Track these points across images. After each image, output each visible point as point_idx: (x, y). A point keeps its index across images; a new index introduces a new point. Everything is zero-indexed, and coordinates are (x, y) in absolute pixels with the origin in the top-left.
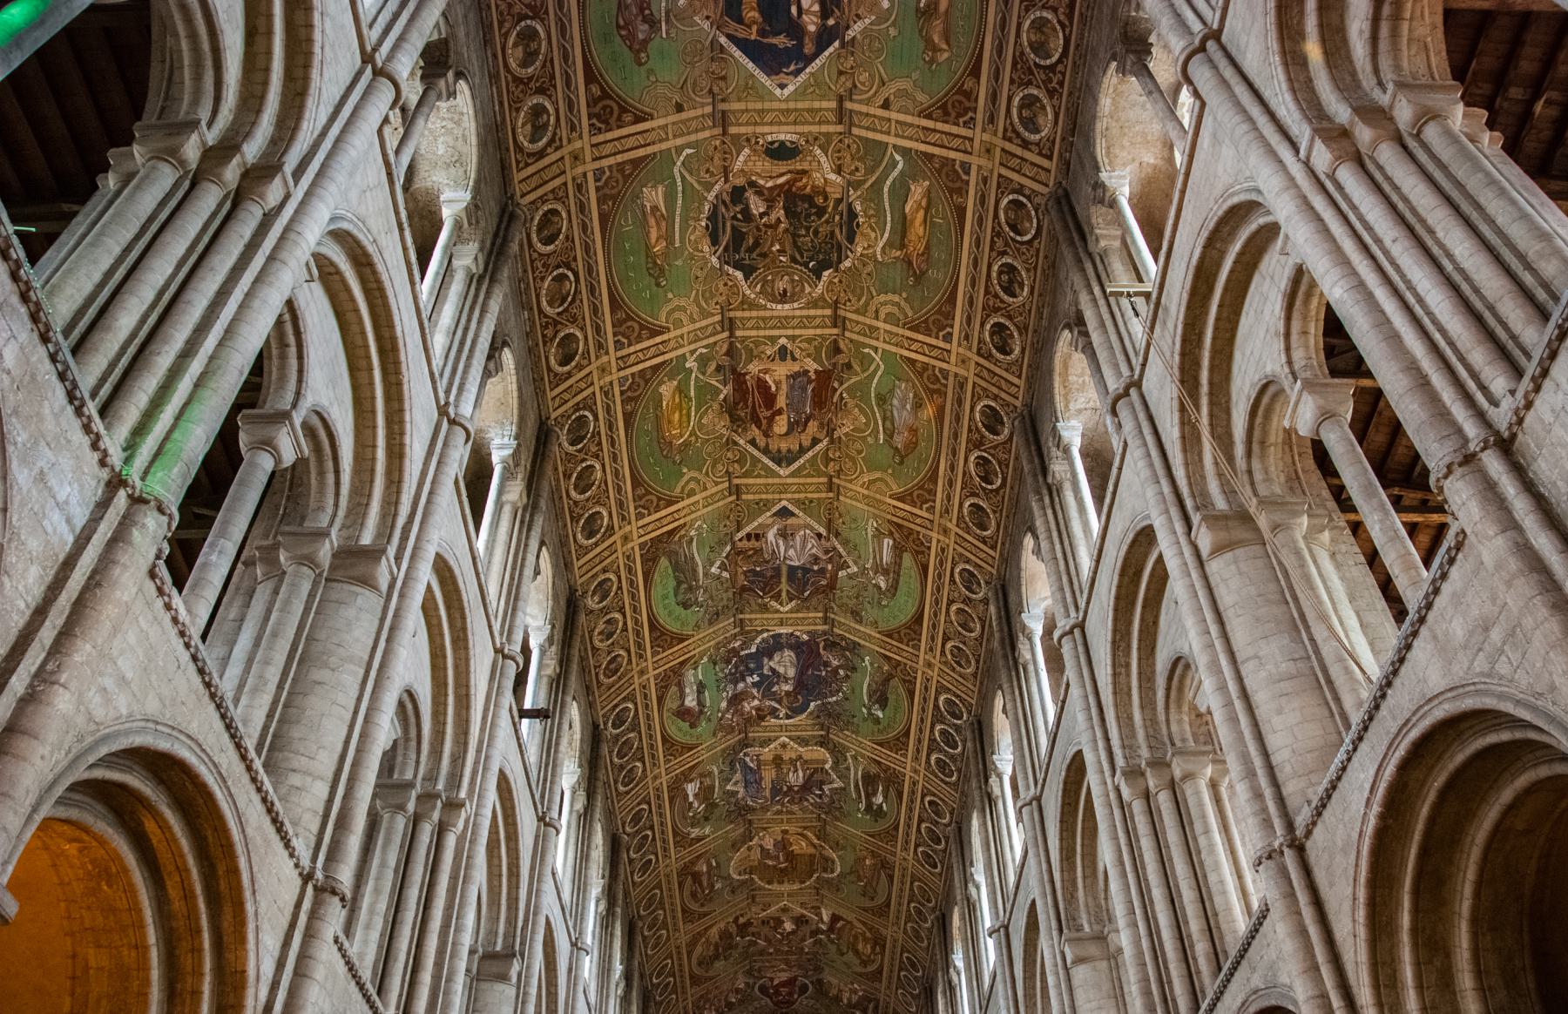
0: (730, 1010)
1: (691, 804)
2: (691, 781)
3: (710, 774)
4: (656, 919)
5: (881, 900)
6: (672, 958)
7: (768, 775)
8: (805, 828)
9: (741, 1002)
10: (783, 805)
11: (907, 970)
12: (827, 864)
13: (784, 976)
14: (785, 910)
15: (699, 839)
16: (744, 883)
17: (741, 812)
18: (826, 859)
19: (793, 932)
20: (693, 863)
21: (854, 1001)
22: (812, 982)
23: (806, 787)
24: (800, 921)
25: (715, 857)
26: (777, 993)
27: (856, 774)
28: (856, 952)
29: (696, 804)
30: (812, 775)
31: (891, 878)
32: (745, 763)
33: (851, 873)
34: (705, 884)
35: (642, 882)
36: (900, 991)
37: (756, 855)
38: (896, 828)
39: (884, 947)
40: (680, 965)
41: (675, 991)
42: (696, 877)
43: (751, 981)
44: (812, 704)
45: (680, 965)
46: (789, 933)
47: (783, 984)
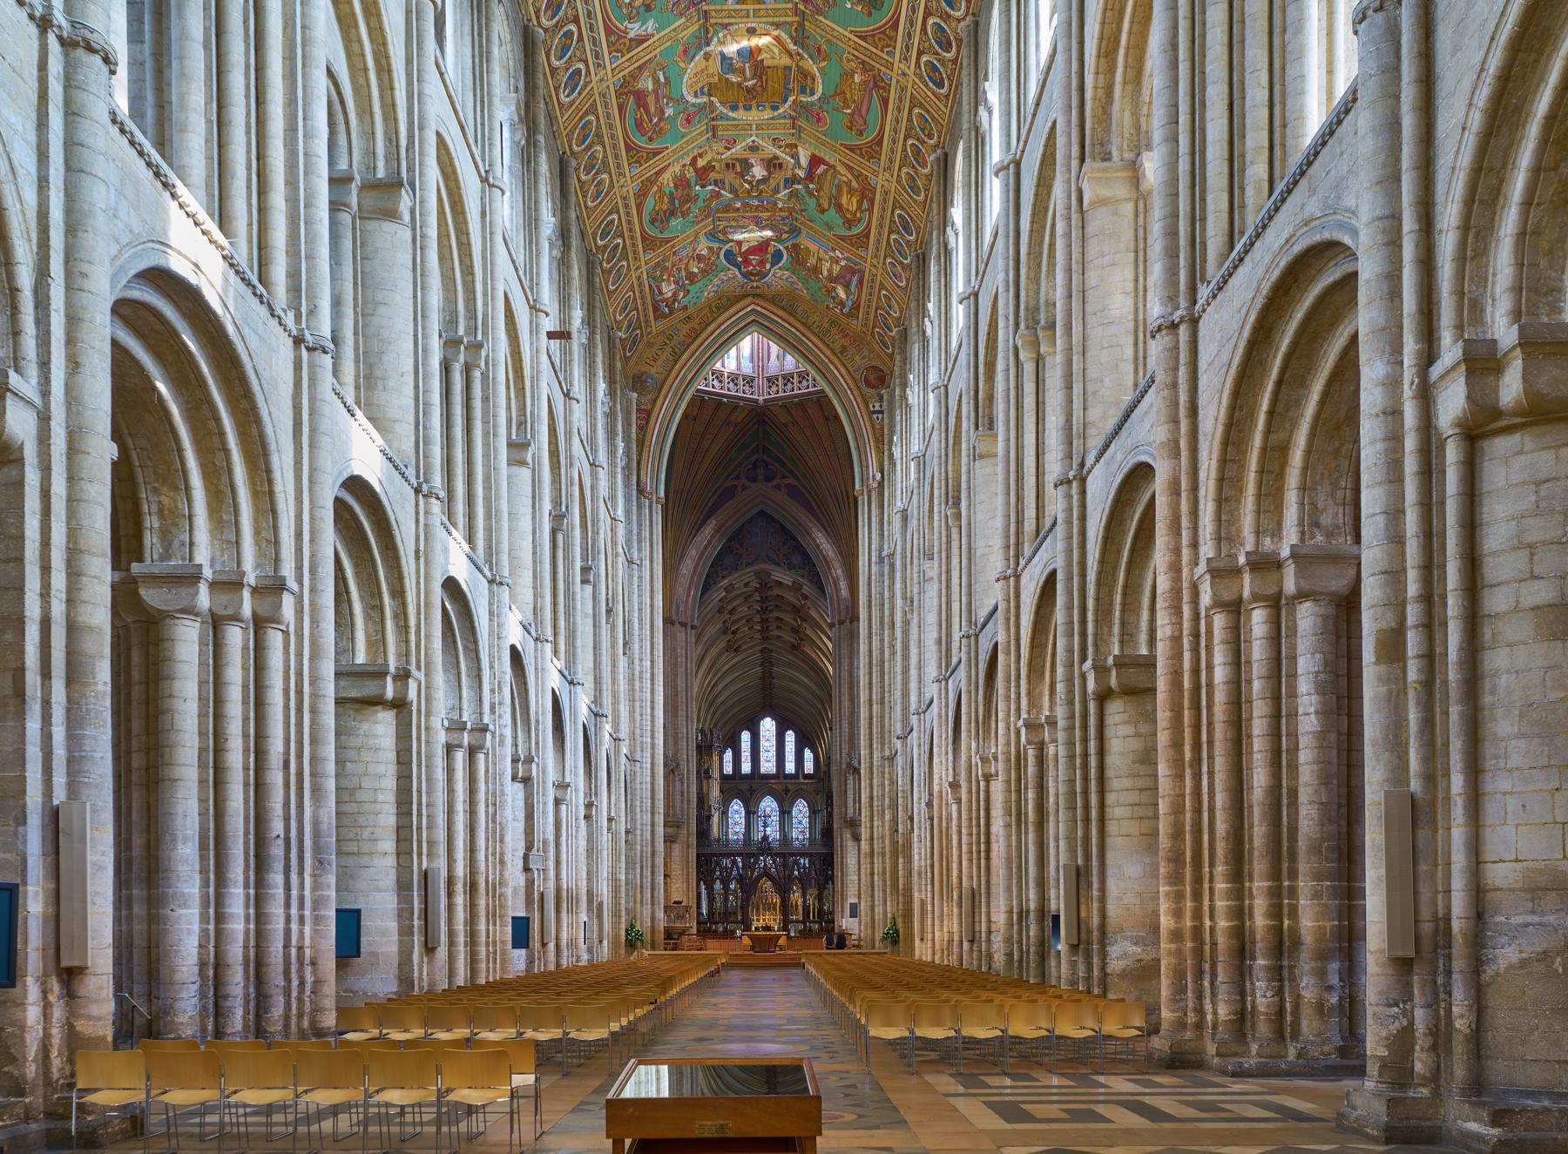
4: (593, 157)
5: (870, 135)
9: (704, 272)
14: (754, 148)
15: (640, 41)
16: (701, 108)
18: (805, 74)
19: (764, 180)
20: (634, 76)
21: (835, 273)
22: (786, 248)
24: (773, 164)
26: (747, 262)
28: (839, 208)
31: (885, 102)
33: (836, 94)
34: (652, 109)
35: (571, 104)
37: (715, 66)
38: (895, 26)
39: (872, 202)
40: (629, 222)
42: (640, 97)
43: (716, 245)
45: (629, 222)
47: (752, 251)
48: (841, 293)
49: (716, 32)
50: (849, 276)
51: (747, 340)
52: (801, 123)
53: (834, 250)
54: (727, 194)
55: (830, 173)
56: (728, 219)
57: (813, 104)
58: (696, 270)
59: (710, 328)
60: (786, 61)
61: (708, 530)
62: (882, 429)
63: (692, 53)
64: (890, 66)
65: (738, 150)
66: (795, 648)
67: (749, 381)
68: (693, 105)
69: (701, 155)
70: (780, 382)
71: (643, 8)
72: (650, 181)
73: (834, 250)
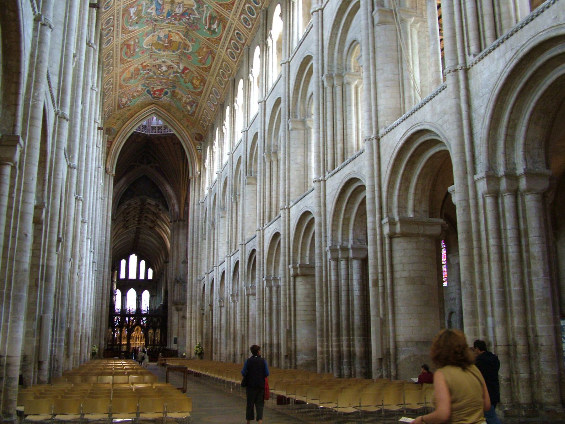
1: (131, 16)
2: (133, 7)
3: (142, 5)
4: (109, 62)
5: (207, 65)
6: (113, 78)
8: (179, 31)
9: (139, 96)
10: (171, 21)
11: (213, 95)
12: (186, 47)
13: (159, 88)
14: (164, 62)
15: (132, 31)
16: (148, 49)
18: (186, 45)
19: (166, 71)
20: (128, 41)
23: (183, 15)
24: (170, 67)
26: (154, 94)
27: (207, 14)
28: (192, 83)
29: (133, 17)
30: (187, 10)
31: (213, 58)
34: (132, 49)
36: (208, 102)
37: (156, 38)
38: (220, 39)
39: (204, 84)
41: (112, 91)
42: (128, 46)
43: (144, 88)
47: (158, 91)
49: (157, 30)
50: (192, 103)
52: (183, 57)
54: (151, 74)
55: (190, 73)
57: (187, 53)
58: (135, 95)
60: (180, 40)
61: (122, 182)
64: (217, 49)
65: (158, 62)
67: (144, 127)
69: (145, 62)
70: (157, 129)
72: (126, 69)
73: (188, 95)
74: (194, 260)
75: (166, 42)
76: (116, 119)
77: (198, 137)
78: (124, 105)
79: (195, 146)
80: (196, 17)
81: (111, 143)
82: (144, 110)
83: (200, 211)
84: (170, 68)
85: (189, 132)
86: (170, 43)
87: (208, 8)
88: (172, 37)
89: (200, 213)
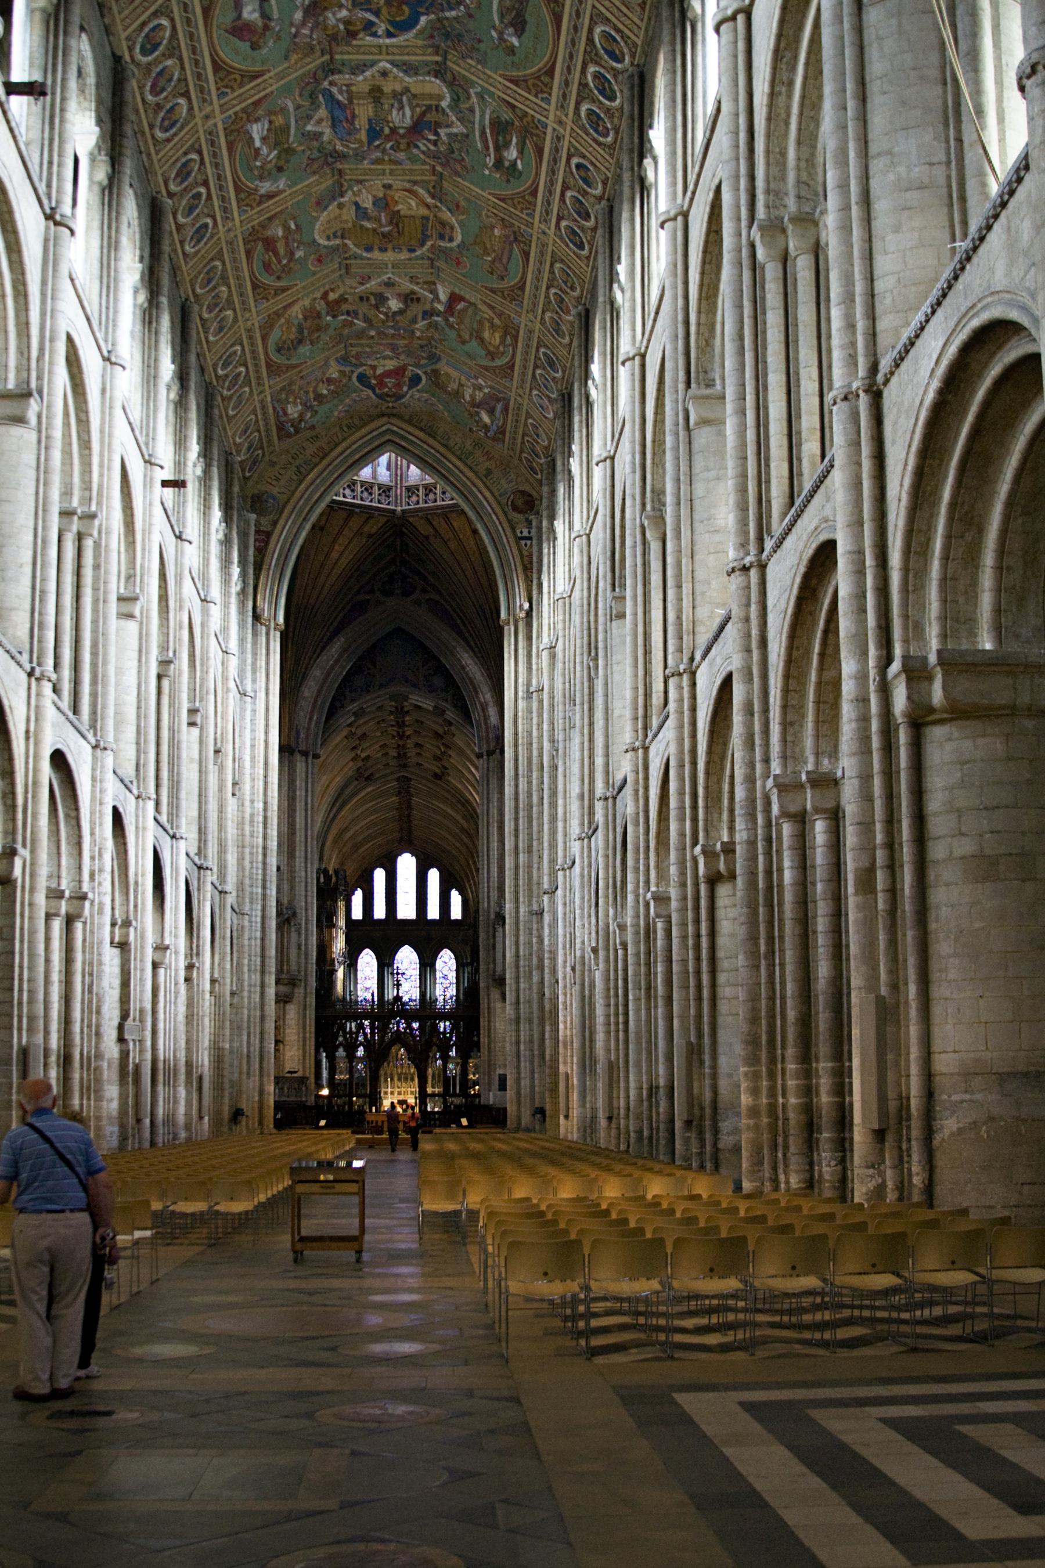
0: (320, 403)
2: (257, 120)
3: (283, 110)
4: (217, 296)
7: (364, 112)
8: (415, 183)
9: (335, 394)
10: (384, 151)
11: (544, 369)
12: (444, 231)
13: (390, 365)
14: (389, 284)
15: (270, 196)
16: (335, 249)
17: (330, 158)
18: (443, 224)
19: (401, 312)
20: (263, 226)
22: (425, 373)
23: (417, 128)
24: (409, 298)
25: (294, 218)
26: (381, 384)
27: (482, 117)
29: (265, 150)
30: (423, 114)
31: (526, 255)
32: (331, 95)
33: (475, 243)
34: (282, 251)
35: (197, 253)
37: (349, 215)
38: (534, 193)
39: (516, 338)
40: (253, 352)
41: (247, 382)
42: (269, 244)
43: (347, 369)
44: (423, 19)
46: (395, 313)
47: (388, 374)
48: (486, 418)
49: (350, 187)
50: (492, 403)
51: (384, 459)
53: (476, 378)
54: (359, 323)
55: (470, 310)
56: (362, 345)
57: (451, 249)
58: (325, 392)
59: (339, 449)
62: (531, 556)
63: (325, 203)
65: (372, 285)
66: (436, 776)
67: (385, 490)
68: (325, 247)
71: (274, 171)
73: (476, 378)
74: (521, 856)
75: (384, 220)
76: (277, 467)
77: (520, 503)
78: (296, 425)
79: (513, 529)
80: (455, 130)
81: (268, 535)
82: (358, 434)
83: (535, 714)
84: (412, 300)
85: (495, 490)
86: (397, 225)
87: (483, 98)
88: (396, 202)
89: (535, 721)
